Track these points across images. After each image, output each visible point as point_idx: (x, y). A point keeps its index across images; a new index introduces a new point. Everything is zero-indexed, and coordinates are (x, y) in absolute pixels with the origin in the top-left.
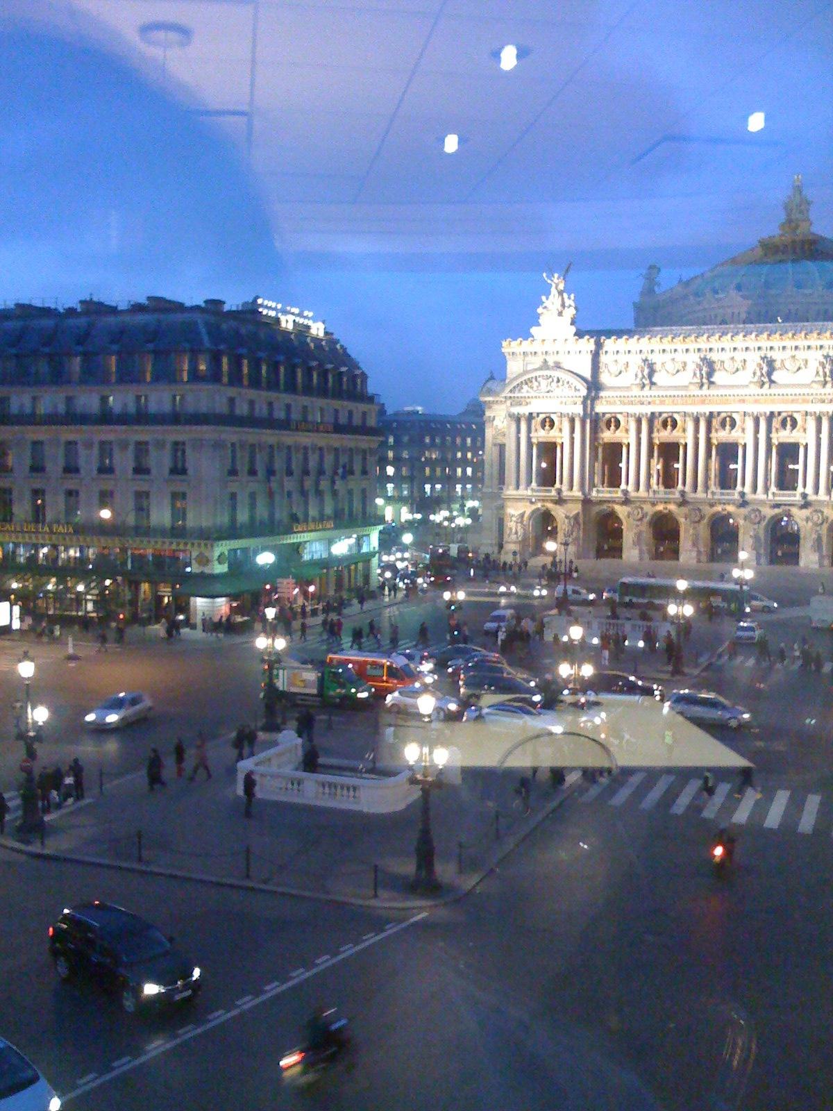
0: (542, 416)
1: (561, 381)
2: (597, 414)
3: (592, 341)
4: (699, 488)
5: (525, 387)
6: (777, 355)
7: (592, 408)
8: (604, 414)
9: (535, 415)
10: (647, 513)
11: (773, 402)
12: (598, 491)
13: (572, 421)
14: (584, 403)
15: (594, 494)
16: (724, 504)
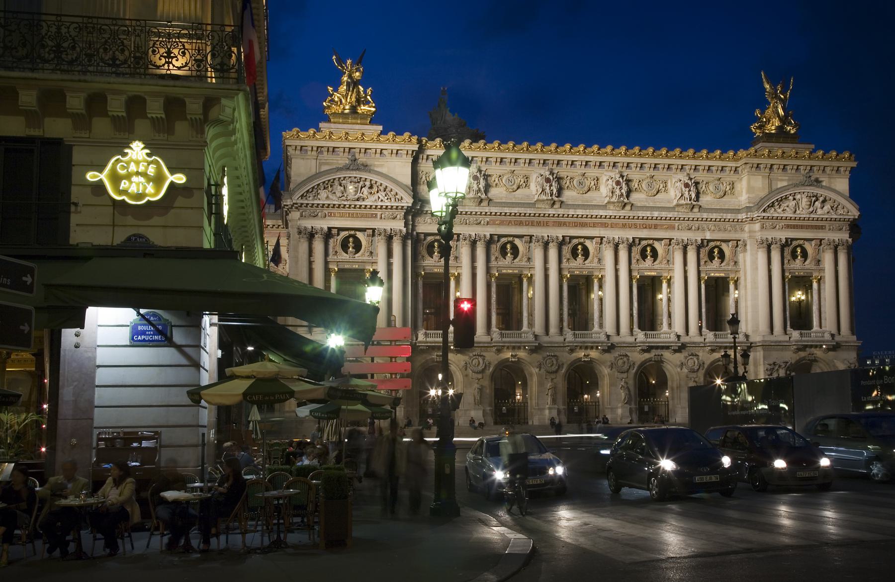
0: (344, 234)
1: (375, 189)
2: (417, 233)
3: (414, 139)
4: (553, 329)
5: (323, 194)
6: (634, 175)
7: (414, 226)
8: (427, 235)
9: (334, 231)
10: (490, 363)
11: (635, 226)
12: (426, 335)
13: (389, 239)
14: (405, 217)
15: (421, 337)
16: (586, 348)
